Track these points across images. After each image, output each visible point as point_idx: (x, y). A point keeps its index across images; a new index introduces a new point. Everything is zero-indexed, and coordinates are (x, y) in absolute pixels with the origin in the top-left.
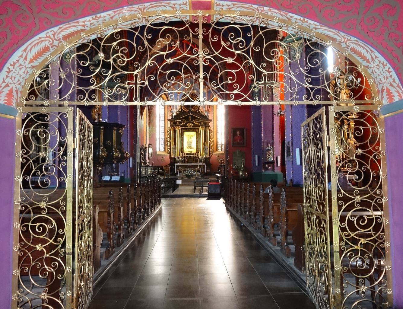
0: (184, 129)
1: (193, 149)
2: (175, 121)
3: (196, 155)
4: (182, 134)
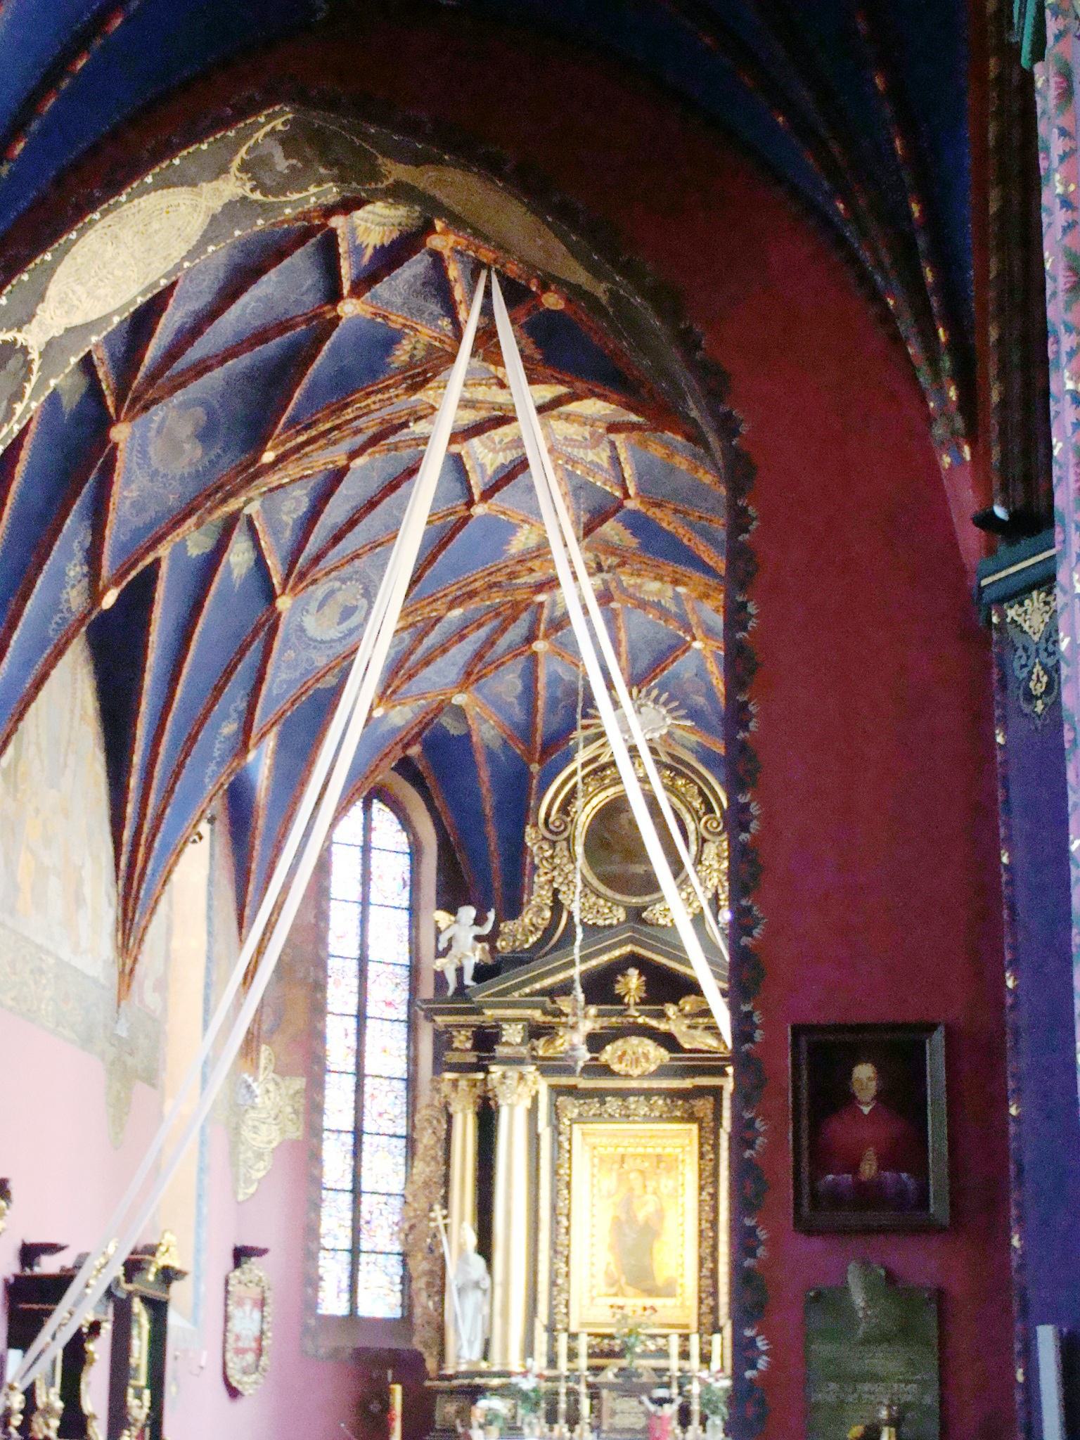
0: (571, 1091)
1: (668, 1291)
2: (488, 1012)
3: (685, 1355)
4: (557, 1146)
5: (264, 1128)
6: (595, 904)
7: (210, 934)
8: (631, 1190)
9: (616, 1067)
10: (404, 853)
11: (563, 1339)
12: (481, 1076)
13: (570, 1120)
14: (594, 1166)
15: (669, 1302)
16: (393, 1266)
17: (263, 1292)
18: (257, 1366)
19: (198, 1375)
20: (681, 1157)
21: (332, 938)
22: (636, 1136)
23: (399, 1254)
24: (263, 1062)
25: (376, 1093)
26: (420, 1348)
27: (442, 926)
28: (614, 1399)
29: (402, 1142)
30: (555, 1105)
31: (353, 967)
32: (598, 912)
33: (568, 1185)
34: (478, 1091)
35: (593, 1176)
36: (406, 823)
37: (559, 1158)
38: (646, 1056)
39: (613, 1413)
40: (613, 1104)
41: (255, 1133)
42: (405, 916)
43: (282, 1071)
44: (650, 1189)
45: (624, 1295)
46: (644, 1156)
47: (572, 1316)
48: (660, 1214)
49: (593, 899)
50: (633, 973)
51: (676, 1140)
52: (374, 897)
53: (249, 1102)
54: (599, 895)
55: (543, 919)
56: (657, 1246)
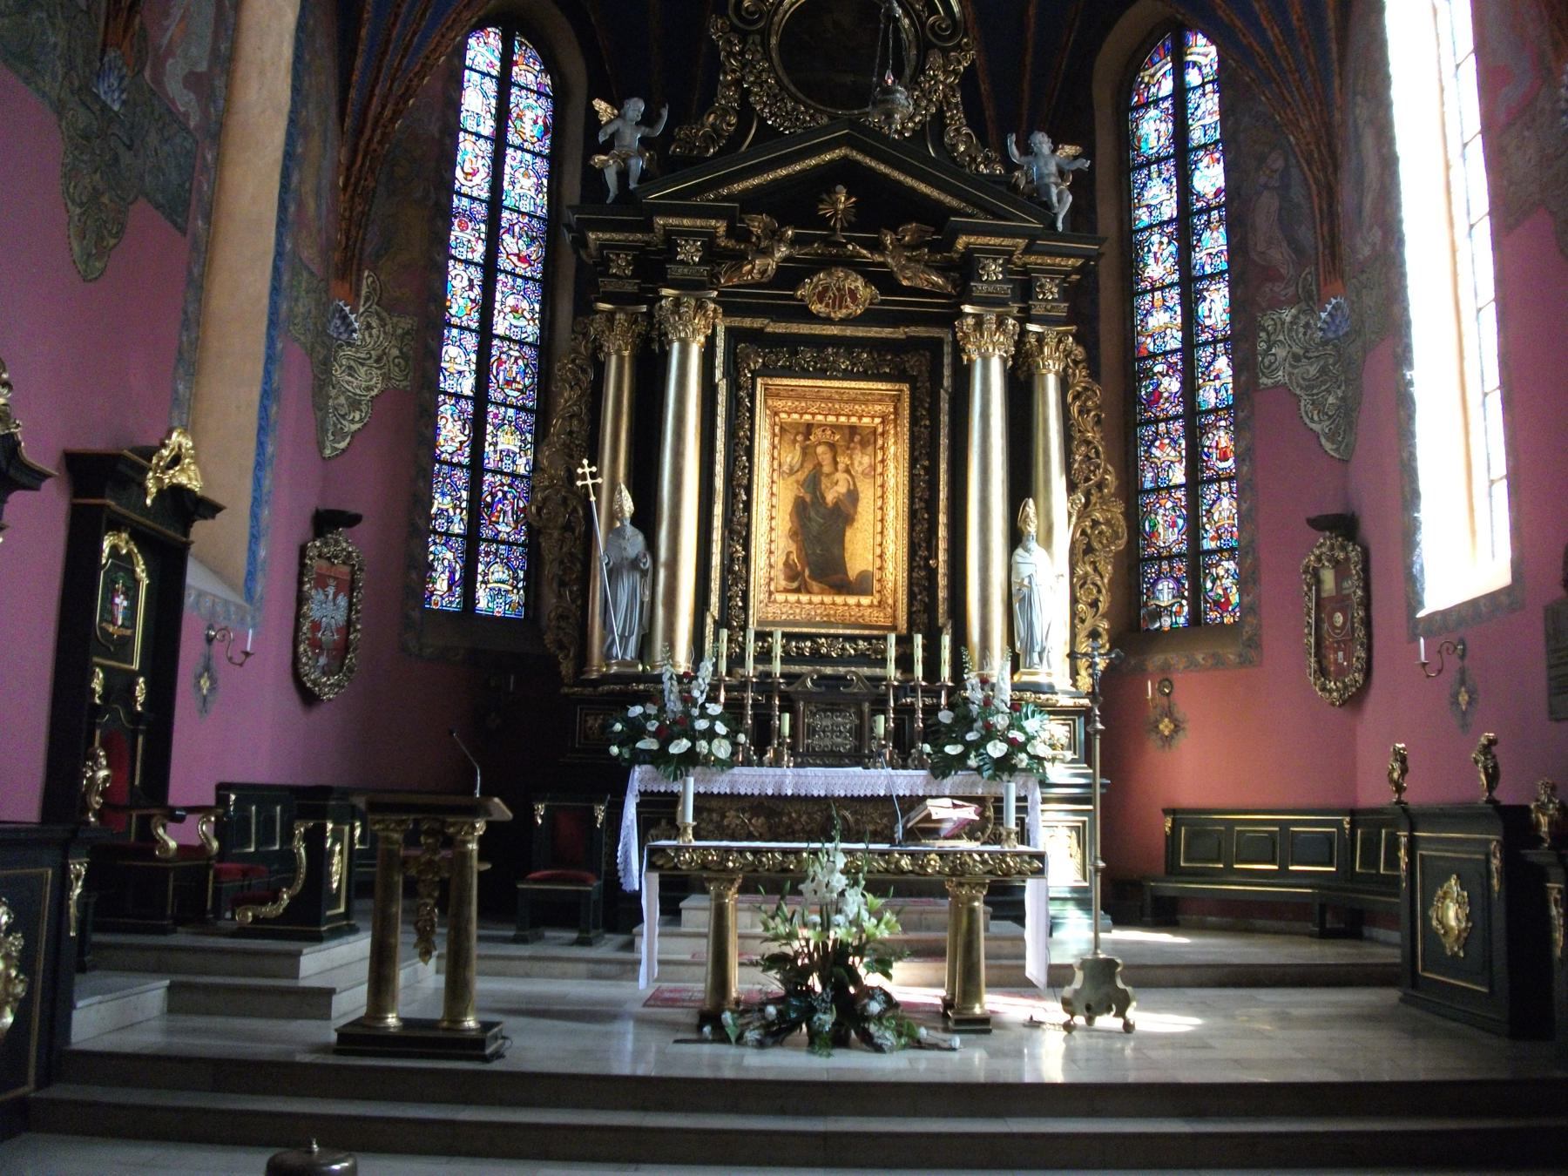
0: (757, 338)
1: (861, 586)
3: (905, 662)
5: (363, 370)
6: (794, 109)
7: (296, 89)
8: (820, 465)
9: (816, 308)
10: (547, 96)
11: (751, 635)
12: (644, 308)
13: (750, 371)
14: (774, 435)
15: (865, 600)
16: (517, 558)
17: (353, 573)
18: (342, 664)
19: (241, 665)
20: (880, 430)
21: (459, 173)
22: (829, 399)
23: (522, 545)
24: (364, 291)
25: (504, 357)
26: (553, 649)
27: (604, 119)
28: (813, 714)
29: (531, 419)
30: (735, 354)
31: (481, 210)
32: (797, 119)
33: (750, 452)
34: (641, 328)
35: (774, 447)
36: (550, 65)
37: (737, 418)
38: (853, 293)
39: (812, 731)
40: (807, 356)
41: (350, 375)
42: (542, 166)
43: (388, 305)
44: (841, 466)
45: (809, 592)
46: (835, 428)
47: (751, 612)
48: (853, 496)
49: (790, 105)
50: (840, 188)
51: (878, 408)
52: (512, 138)
53: (344, 336)
54: (796, 102)
55: (729, 124)
56: (849, 534)
